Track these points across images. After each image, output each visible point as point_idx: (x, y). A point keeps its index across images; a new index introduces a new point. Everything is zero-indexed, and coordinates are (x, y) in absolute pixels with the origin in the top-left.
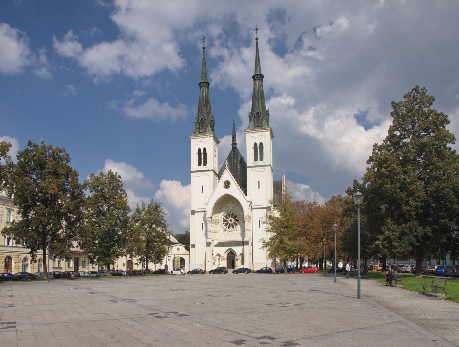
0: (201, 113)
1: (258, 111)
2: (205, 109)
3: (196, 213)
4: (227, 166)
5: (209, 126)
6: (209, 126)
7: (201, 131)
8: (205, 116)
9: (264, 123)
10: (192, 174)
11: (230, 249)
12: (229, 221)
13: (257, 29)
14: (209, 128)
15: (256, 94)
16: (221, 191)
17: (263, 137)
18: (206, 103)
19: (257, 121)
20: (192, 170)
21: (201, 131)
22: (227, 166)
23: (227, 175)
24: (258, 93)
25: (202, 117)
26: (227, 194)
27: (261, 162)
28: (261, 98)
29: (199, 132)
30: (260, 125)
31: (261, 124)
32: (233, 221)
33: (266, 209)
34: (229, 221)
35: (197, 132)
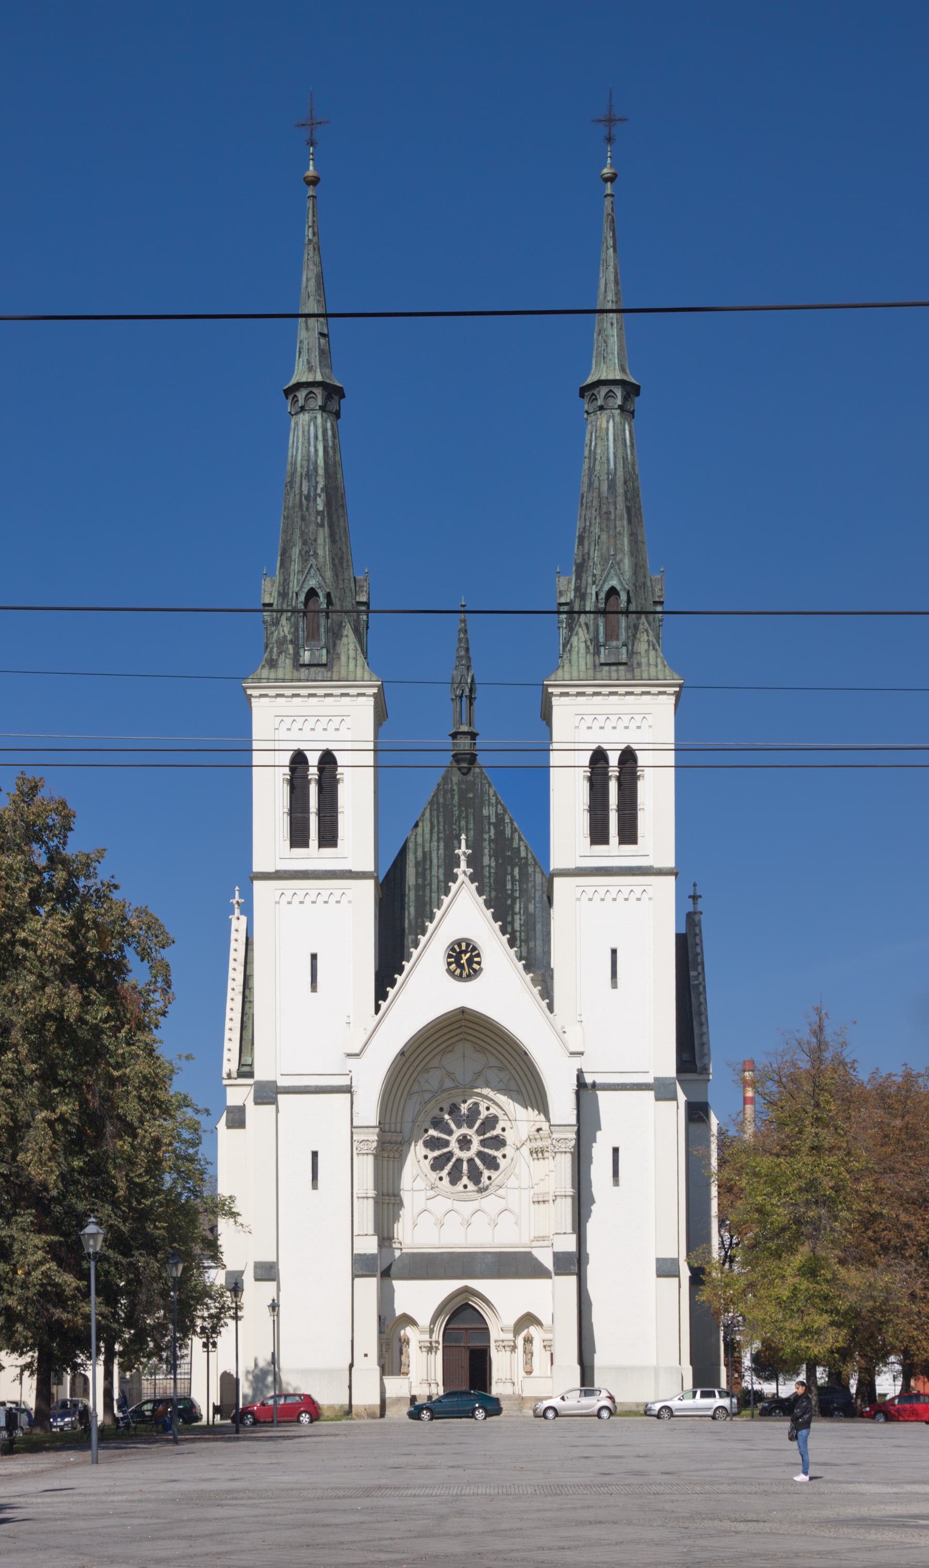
0: (304, 557)
1: (614, 582)
2: (323, 536)
3: (280, 1097)
4: (463, 864)
5: (348, 631)
6: (348, 631)
7: (306, 657)
8: (329, 574)
9: (642, 647)
10: (258, 885)
11: (466, 1290)
12: (454, 1146)
13: (610, 121)
14: (349, 641)
15: (605, 487)
16: (427, 991)
17: (639, 719)
18: (328, 504)
19: (608, 637)
20: (257, 867)
21: (306, 657)
22: (463, 864)
23: (464, 913)
24: (612, 485)
25: (312, 583)
26: (463, 1011)
27: (628, 849)
28: (628, 509)
29: (298, 665)
30: (624, 658)
31: (631, 654)
32: (475, 1146)
33: (651, 1094)
34: (454, 1146)
35: (286, 663)
